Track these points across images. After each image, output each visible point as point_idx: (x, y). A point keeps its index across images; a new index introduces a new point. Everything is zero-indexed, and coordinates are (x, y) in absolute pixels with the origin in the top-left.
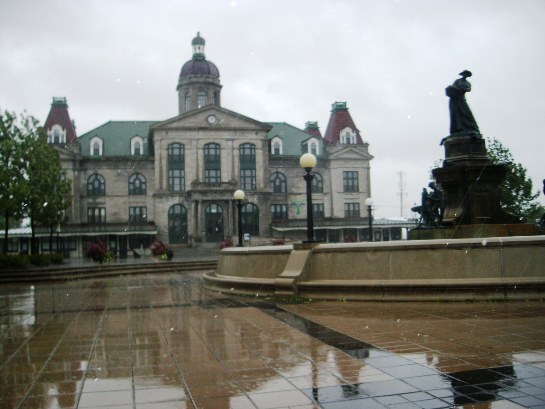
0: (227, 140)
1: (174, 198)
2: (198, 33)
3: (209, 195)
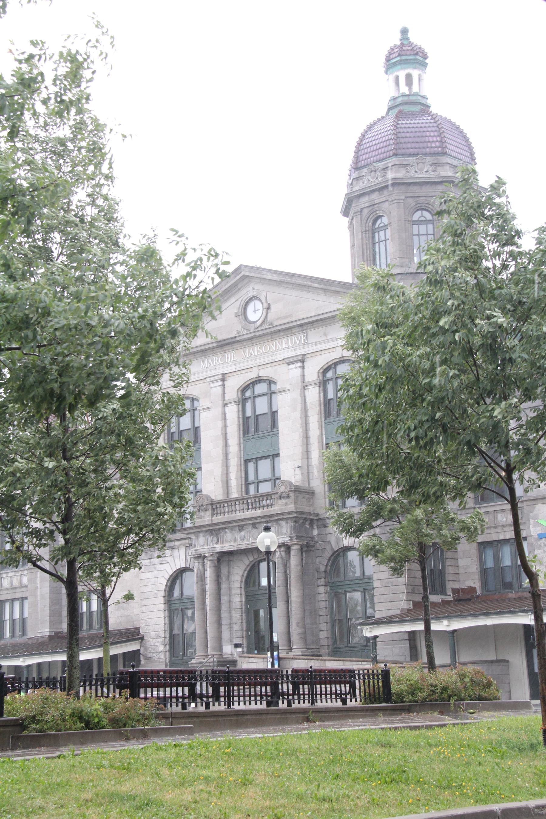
0: (290, 362)
1: (176, 552)
2: (404, 32)
3: (228, 535)
